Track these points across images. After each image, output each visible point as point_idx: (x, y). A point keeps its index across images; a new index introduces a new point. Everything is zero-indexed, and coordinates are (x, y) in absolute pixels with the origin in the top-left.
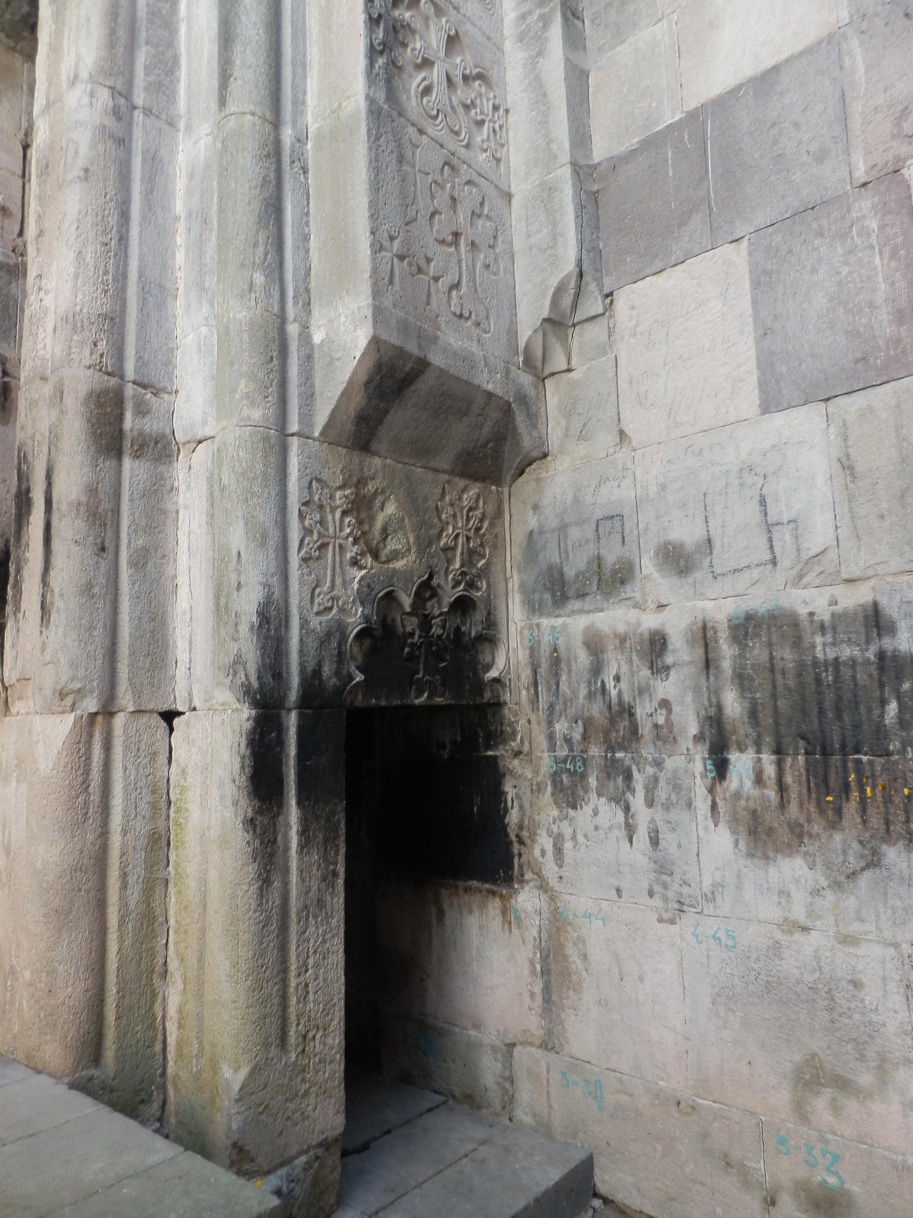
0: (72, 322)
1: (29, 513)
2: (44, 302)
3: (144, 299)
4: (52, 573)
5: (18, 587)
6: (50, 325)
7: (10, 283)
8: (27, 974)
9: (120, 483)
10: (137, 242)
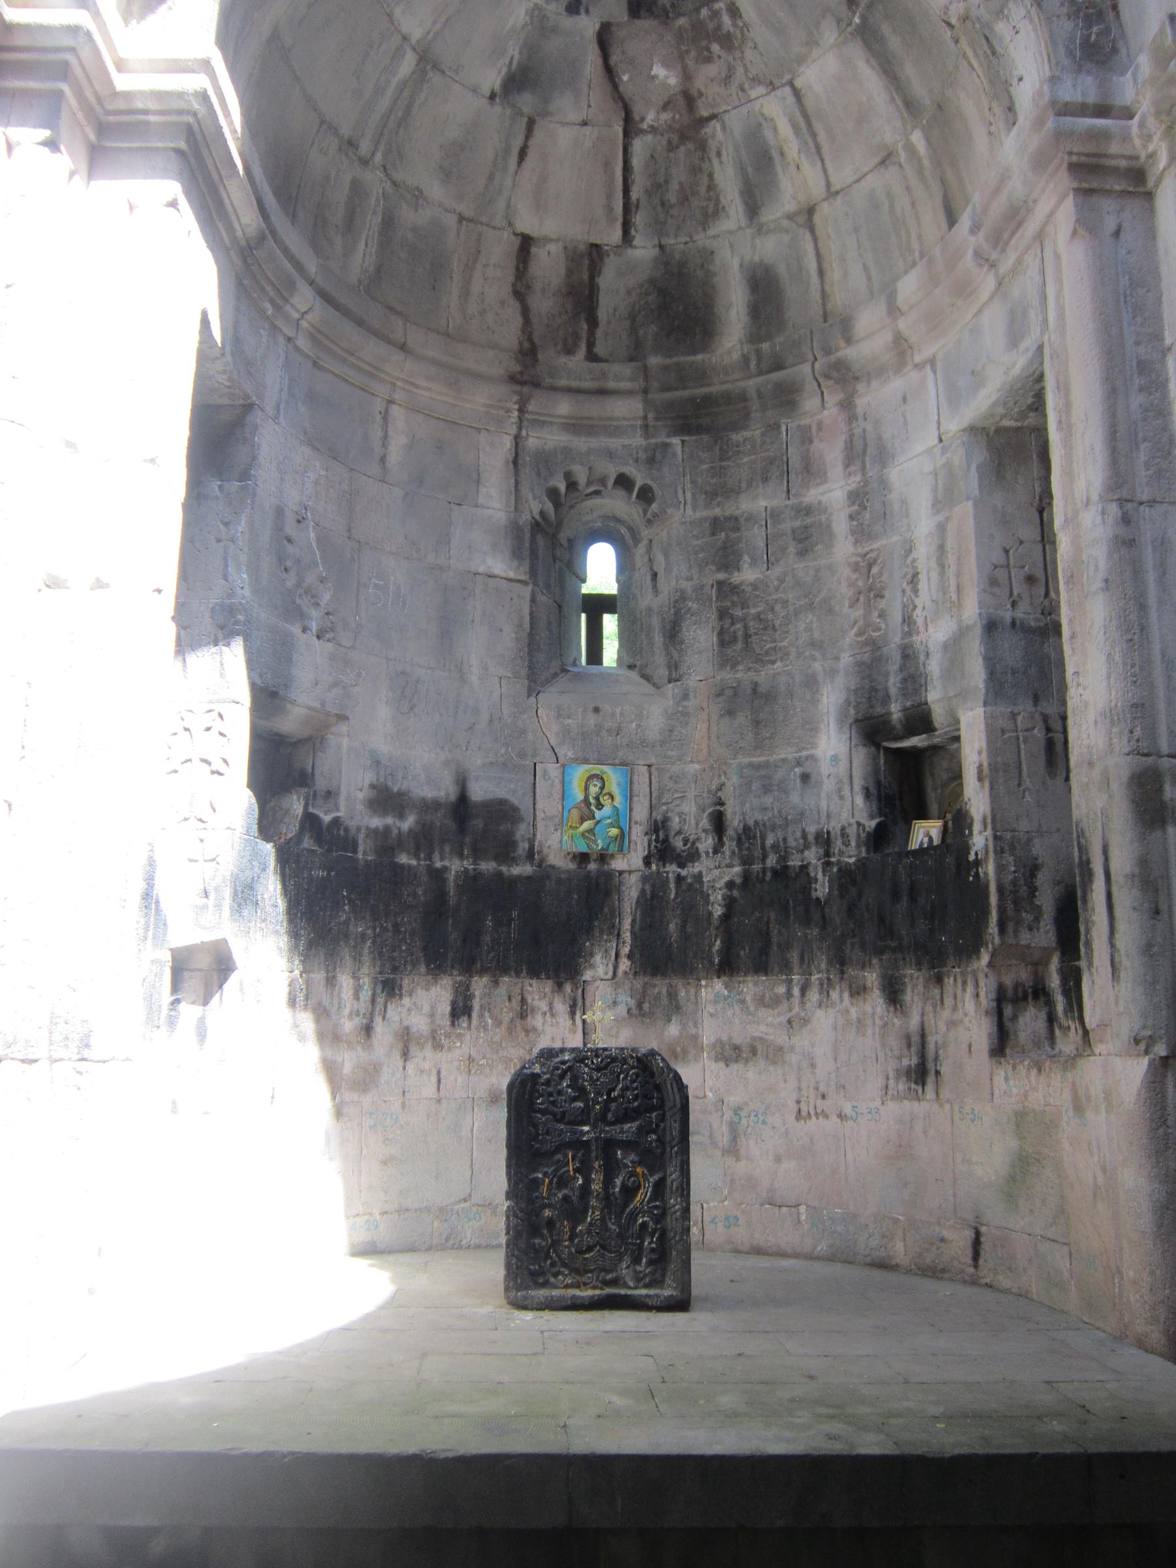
0: (1110, 717)
1: (1091, 881)
2: (1084, 697)
3: (1169, 677)
4: (1117, 936)
5: (1088, 944)
6: (1091, 717)
7: (1043, 643)
8: (1131, 1273)
9: (1166, 850)
10: (1156, 627)
